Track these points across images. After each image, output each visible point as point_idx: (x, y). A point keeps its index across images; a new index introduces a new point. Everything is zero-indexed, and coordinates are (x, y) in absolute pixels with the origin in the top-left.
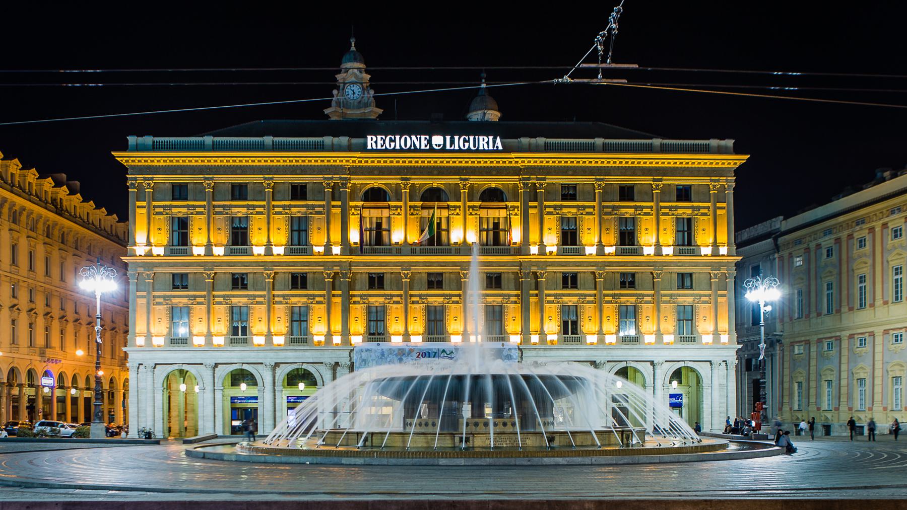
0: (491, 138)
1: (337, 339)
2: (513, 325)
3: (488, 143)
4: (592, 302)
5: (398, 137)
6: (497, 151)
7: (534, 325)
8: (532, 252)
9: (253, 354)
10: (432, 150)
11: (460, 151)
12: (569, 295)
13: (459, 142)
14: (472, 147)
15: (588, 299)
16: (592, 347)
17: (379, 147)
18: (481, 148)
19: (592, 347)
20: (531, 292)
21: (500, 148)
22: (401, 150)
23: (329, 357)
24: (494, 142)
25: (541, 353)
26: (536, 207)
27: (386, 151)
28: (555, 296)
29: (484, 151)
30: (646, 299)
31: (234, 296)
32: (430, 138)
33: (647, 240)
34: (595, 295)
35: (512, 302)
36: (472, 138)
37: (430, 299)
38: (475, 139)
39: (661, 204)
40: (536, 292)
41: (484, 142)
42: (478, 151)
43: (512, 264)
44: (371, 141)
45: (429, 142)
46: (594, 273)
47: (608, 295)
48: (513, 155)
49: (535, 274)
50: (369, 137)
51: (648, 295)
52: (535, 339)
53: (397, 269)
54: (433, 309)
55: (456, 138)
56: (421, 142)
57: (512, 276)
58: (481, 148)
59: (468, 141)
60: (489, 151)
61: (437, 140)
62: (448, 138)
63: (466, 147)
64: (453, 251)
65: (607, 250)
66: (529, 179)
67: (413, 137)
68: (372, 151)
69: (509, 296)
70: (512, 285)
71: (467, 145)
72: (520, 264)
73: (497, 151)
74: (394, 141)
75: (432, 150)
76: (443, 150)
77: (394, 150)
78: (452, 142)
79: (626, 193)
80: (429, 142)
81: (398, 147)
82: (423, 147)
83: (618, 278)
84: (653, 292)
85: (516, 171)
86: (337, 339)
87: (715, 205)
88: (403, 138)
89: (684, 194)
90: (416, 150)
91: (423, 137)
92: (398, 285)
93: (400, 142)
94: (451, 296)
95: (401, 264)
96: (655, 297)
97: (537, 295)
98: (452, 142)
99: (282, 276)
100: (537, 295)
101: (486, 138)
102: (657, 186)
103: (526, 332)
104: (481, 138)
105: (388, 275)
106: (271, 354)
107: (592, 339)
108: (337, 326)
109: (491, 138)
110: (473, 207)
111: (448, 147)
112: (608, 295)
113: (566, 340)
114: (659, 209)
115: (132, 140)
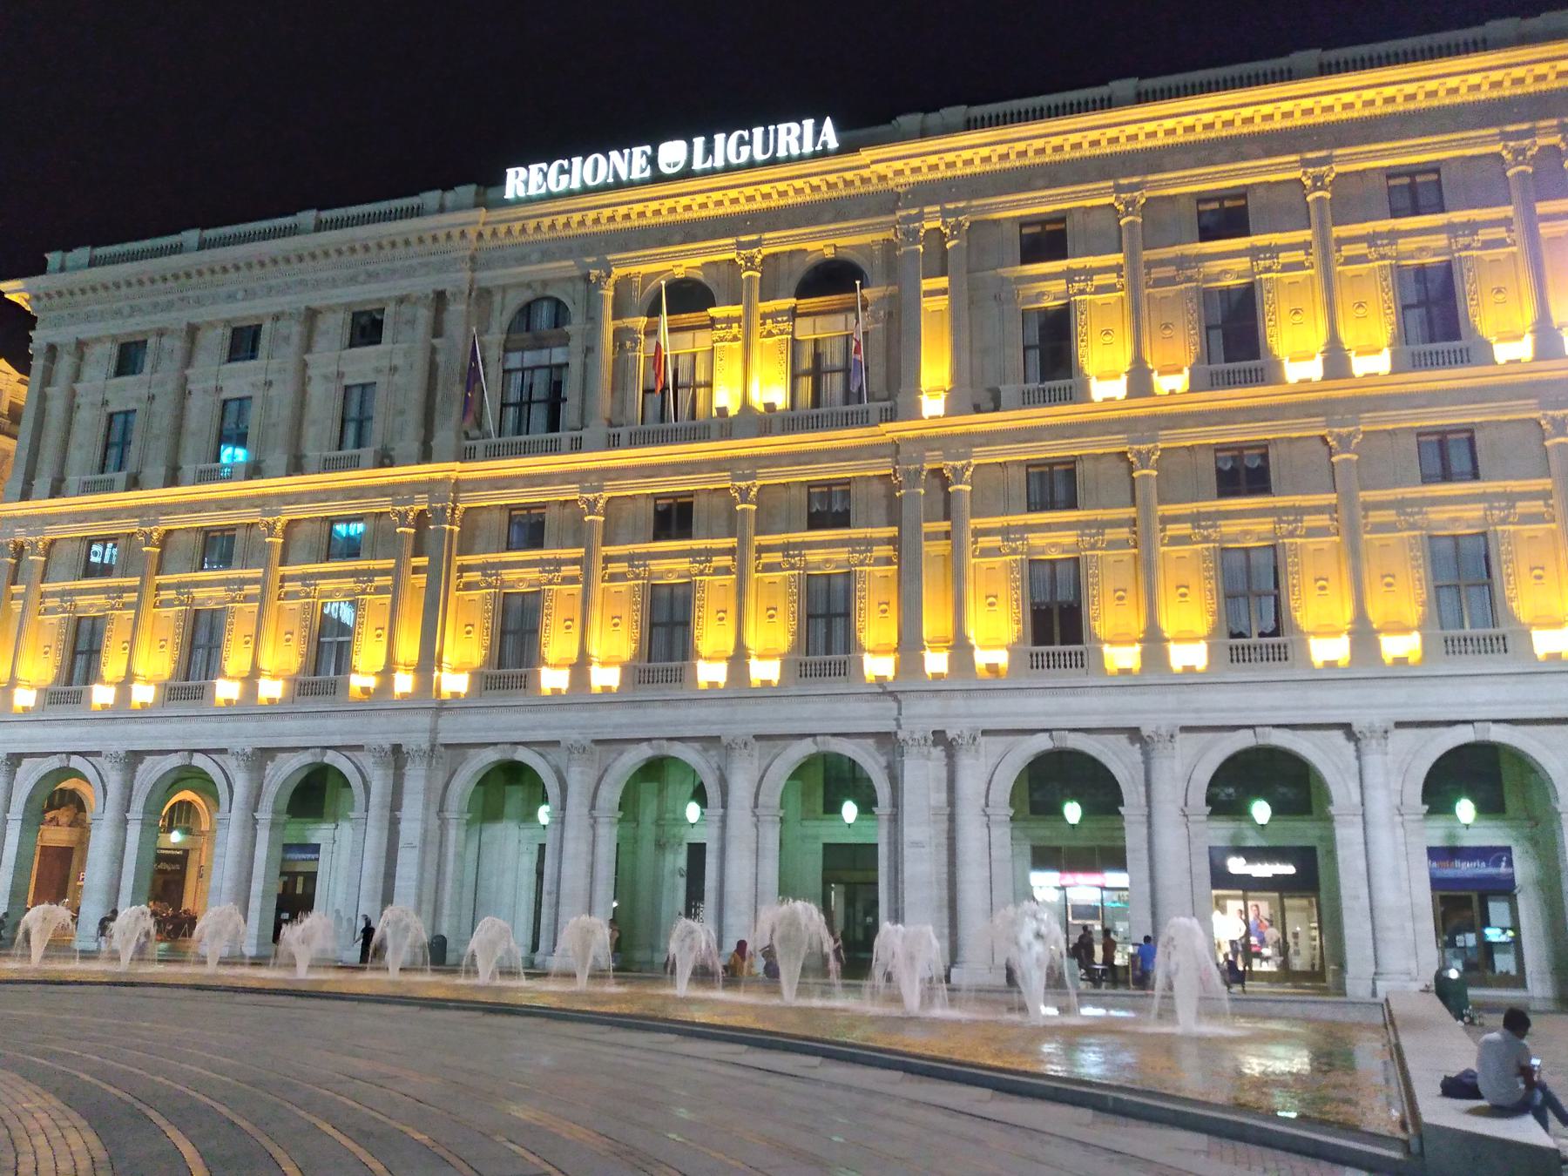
0: (809, 124)
1: (404, 683)
2: (876, 630)
3: (800, 139)
4: (1123, 544)
5: (577, 161)
6: (824, 153)
7: (935, 623)
8: (926, 413)
9: (212, 726)
10: (658, 178)
11: (729, 169)
12: (1048, 527)
13: (726, 147)
14: (759, 156)
15: (1111, 534)
16: (1124, 681)
17: (533, 192)
18: (782, 153)
19: (1126, 682)
20: (928, 527)
21: (833, 144)
22: (586, 191)
23: (380, 733)
24: (817, 132)
25: (958, 704)
26: (943, 292)
27: (551, 197)
28: (1005, 532)
29: (789, 160)
30: (1311, 521)
31: (198, 584)
32: (655, 150)
33: (1295, 345)
34: (1133, 522)
35: (878, 561)
36: (758, 132)
37: (657, 566)
38: (766, 133)
39: (1340, 231)
40: (945, 525)
41: (792, 136)
42: (774, 162)
43: (872, 451)
44: (520, 181)
45: (653, 161)
46: (1122, 455)
47: (1176, 519)
48: (866, 155)
49: (937, 473)
50: (511, 172)
51: (1318, 510)
52: (936, 662)
53: (570, 493)
54: (665, 592)
55: (719, 138)
56: (630, 162)
57: (879, 489)
58: (782, 153)
59: (750, 143)
60: (801, 158)
61: (672, 153)
62: (699, 142)
63: (744, 158)
64: (714, 432)
65: (1162, 384)
66: (920, 217)
67: (614, 155)
68: (519, 202)
69: (869, 543)
70: (880, 512)
71: (745, 150)
72: (895, 448)
73: (824, 153)
74: (569, 172)
75: (658, 178)
76: (687, 173)
77: (570, 194)
78: (709, 150)
79: (1226, 218)
80: (653, 161)
81: (576, 185)
82: (636, 175)
83: (1208, 464)
84: (1330, 498)
85: (885, 202)
86: (404, 683)
87: (1532, 210)
88: (591, 159)
89: (1416, 192)
90: (619, 185)
91: (637, 151)
92: (578, 533)
93: (585, 170)
94: (709, 553)
95: (579, 477)
96: (1342, 514)
97: (947, 535)
98: (709, 150)
99: (306, 527)
100: (947, 535)
101: (794, 126)
102: (1316, 178)
103: (909, 645)
104: (782, 127)
105: (555, 510)
106: (250, 726)
107: (1122, 657)
108: (409, 648)
109: (809, 124)
110: (773, 315)
111: (698, 165)
112: (1176, 519)
113: (1036, 663)
114: (1327, 248)
115: (53, 258)
